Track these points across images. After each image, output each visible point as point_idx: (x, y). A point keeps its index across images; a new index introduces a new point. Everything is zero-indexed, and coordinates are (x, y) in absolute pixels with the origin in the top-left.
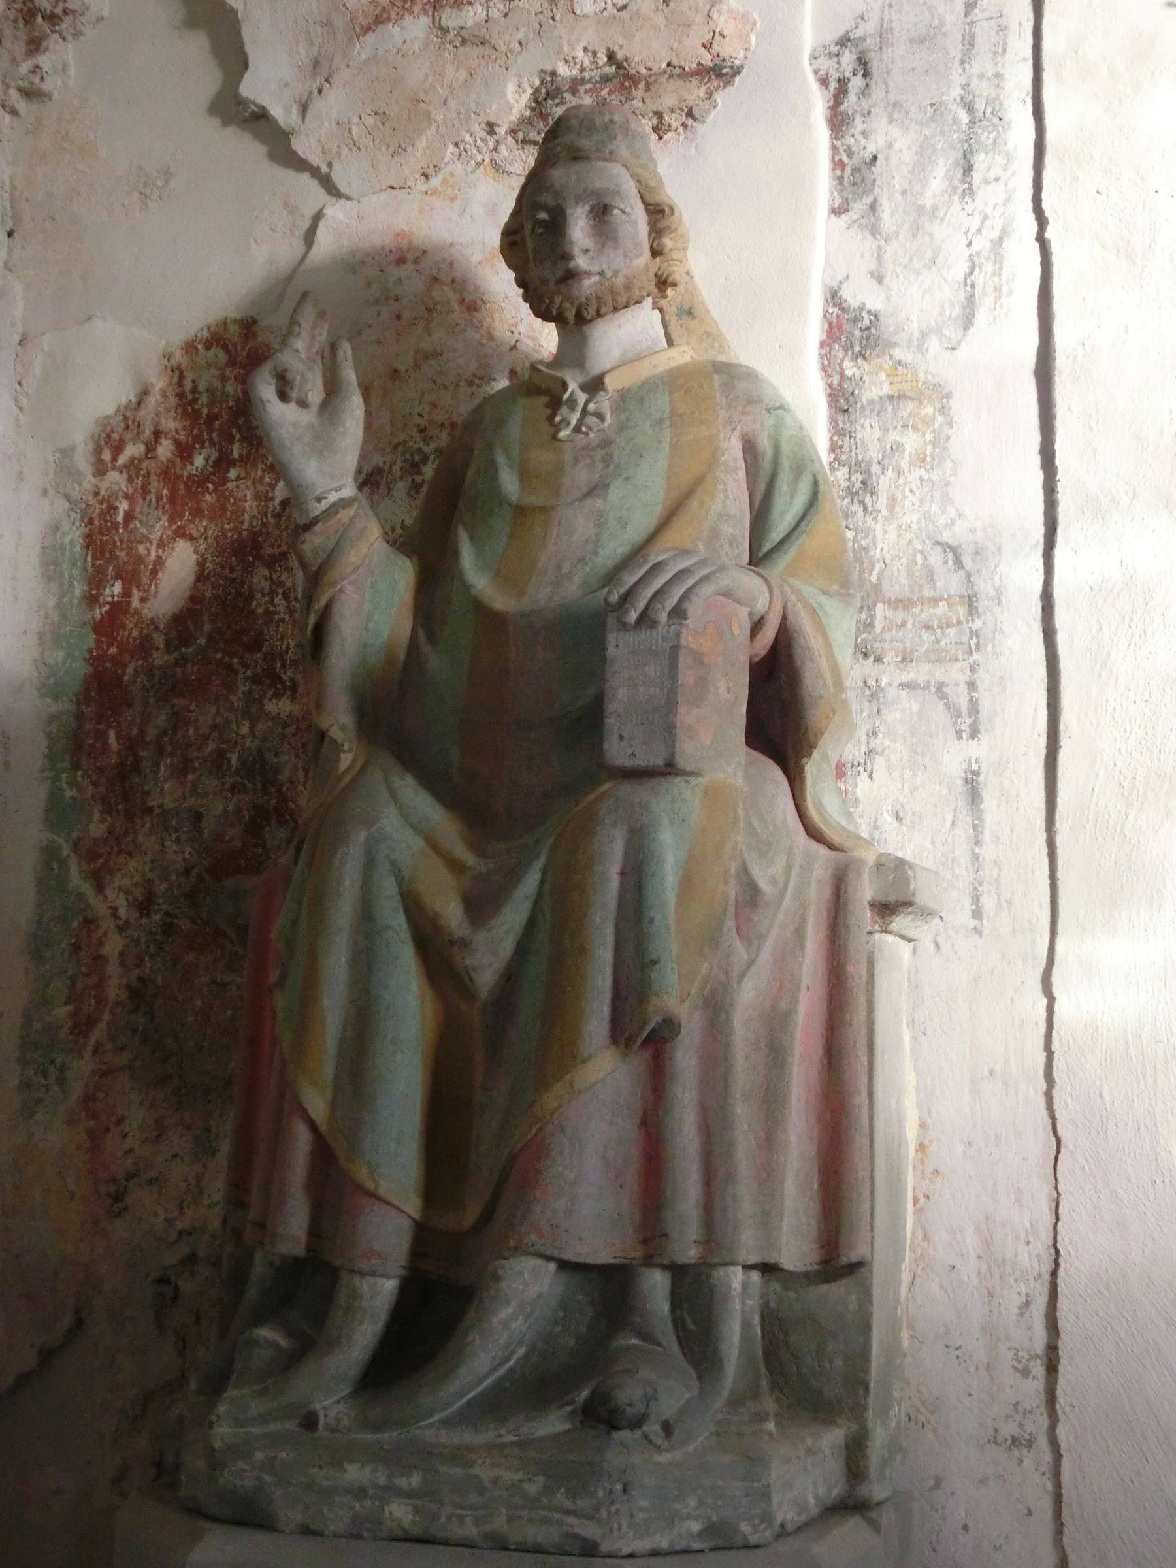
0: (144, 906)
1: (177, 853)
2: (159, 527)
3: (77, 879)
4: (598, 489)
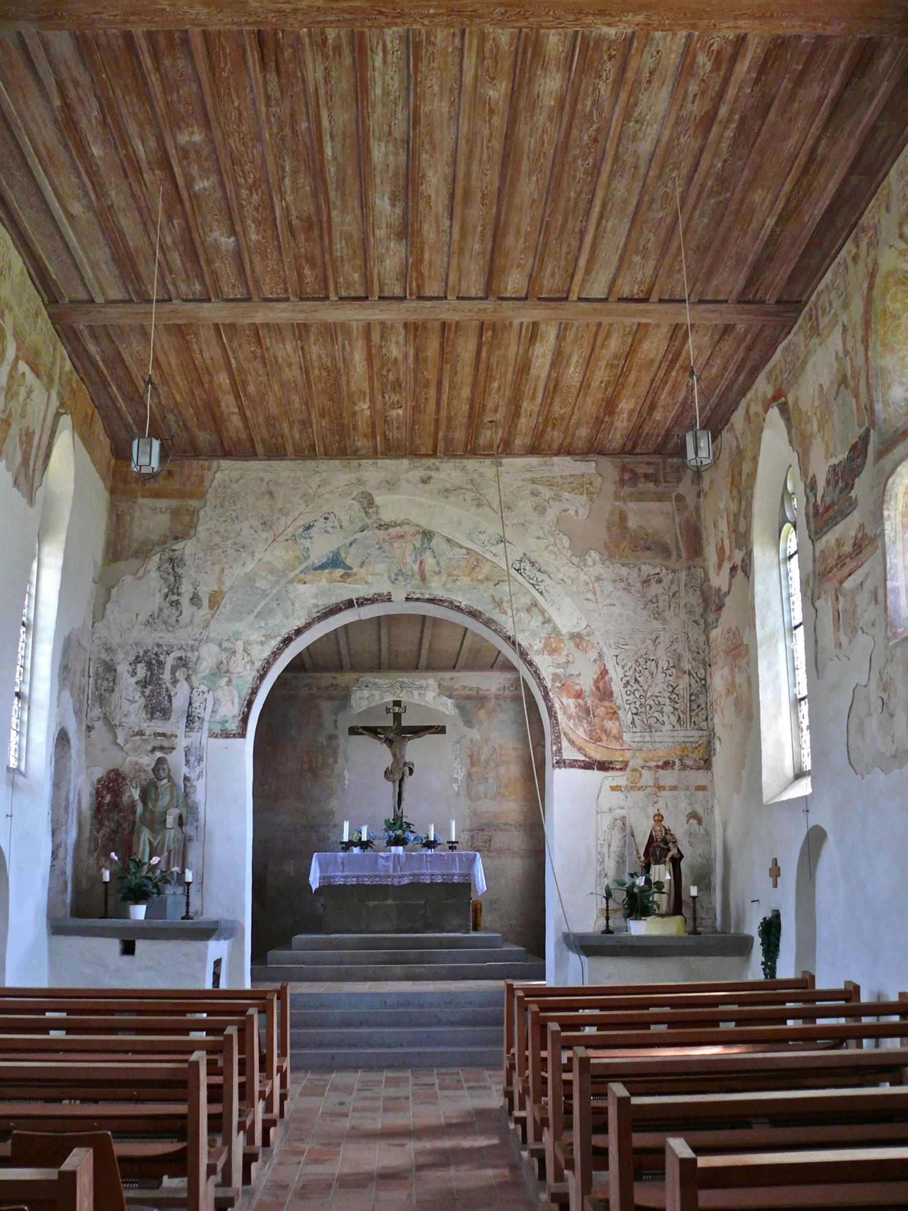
1: (108, 830)
3: (95, 832)
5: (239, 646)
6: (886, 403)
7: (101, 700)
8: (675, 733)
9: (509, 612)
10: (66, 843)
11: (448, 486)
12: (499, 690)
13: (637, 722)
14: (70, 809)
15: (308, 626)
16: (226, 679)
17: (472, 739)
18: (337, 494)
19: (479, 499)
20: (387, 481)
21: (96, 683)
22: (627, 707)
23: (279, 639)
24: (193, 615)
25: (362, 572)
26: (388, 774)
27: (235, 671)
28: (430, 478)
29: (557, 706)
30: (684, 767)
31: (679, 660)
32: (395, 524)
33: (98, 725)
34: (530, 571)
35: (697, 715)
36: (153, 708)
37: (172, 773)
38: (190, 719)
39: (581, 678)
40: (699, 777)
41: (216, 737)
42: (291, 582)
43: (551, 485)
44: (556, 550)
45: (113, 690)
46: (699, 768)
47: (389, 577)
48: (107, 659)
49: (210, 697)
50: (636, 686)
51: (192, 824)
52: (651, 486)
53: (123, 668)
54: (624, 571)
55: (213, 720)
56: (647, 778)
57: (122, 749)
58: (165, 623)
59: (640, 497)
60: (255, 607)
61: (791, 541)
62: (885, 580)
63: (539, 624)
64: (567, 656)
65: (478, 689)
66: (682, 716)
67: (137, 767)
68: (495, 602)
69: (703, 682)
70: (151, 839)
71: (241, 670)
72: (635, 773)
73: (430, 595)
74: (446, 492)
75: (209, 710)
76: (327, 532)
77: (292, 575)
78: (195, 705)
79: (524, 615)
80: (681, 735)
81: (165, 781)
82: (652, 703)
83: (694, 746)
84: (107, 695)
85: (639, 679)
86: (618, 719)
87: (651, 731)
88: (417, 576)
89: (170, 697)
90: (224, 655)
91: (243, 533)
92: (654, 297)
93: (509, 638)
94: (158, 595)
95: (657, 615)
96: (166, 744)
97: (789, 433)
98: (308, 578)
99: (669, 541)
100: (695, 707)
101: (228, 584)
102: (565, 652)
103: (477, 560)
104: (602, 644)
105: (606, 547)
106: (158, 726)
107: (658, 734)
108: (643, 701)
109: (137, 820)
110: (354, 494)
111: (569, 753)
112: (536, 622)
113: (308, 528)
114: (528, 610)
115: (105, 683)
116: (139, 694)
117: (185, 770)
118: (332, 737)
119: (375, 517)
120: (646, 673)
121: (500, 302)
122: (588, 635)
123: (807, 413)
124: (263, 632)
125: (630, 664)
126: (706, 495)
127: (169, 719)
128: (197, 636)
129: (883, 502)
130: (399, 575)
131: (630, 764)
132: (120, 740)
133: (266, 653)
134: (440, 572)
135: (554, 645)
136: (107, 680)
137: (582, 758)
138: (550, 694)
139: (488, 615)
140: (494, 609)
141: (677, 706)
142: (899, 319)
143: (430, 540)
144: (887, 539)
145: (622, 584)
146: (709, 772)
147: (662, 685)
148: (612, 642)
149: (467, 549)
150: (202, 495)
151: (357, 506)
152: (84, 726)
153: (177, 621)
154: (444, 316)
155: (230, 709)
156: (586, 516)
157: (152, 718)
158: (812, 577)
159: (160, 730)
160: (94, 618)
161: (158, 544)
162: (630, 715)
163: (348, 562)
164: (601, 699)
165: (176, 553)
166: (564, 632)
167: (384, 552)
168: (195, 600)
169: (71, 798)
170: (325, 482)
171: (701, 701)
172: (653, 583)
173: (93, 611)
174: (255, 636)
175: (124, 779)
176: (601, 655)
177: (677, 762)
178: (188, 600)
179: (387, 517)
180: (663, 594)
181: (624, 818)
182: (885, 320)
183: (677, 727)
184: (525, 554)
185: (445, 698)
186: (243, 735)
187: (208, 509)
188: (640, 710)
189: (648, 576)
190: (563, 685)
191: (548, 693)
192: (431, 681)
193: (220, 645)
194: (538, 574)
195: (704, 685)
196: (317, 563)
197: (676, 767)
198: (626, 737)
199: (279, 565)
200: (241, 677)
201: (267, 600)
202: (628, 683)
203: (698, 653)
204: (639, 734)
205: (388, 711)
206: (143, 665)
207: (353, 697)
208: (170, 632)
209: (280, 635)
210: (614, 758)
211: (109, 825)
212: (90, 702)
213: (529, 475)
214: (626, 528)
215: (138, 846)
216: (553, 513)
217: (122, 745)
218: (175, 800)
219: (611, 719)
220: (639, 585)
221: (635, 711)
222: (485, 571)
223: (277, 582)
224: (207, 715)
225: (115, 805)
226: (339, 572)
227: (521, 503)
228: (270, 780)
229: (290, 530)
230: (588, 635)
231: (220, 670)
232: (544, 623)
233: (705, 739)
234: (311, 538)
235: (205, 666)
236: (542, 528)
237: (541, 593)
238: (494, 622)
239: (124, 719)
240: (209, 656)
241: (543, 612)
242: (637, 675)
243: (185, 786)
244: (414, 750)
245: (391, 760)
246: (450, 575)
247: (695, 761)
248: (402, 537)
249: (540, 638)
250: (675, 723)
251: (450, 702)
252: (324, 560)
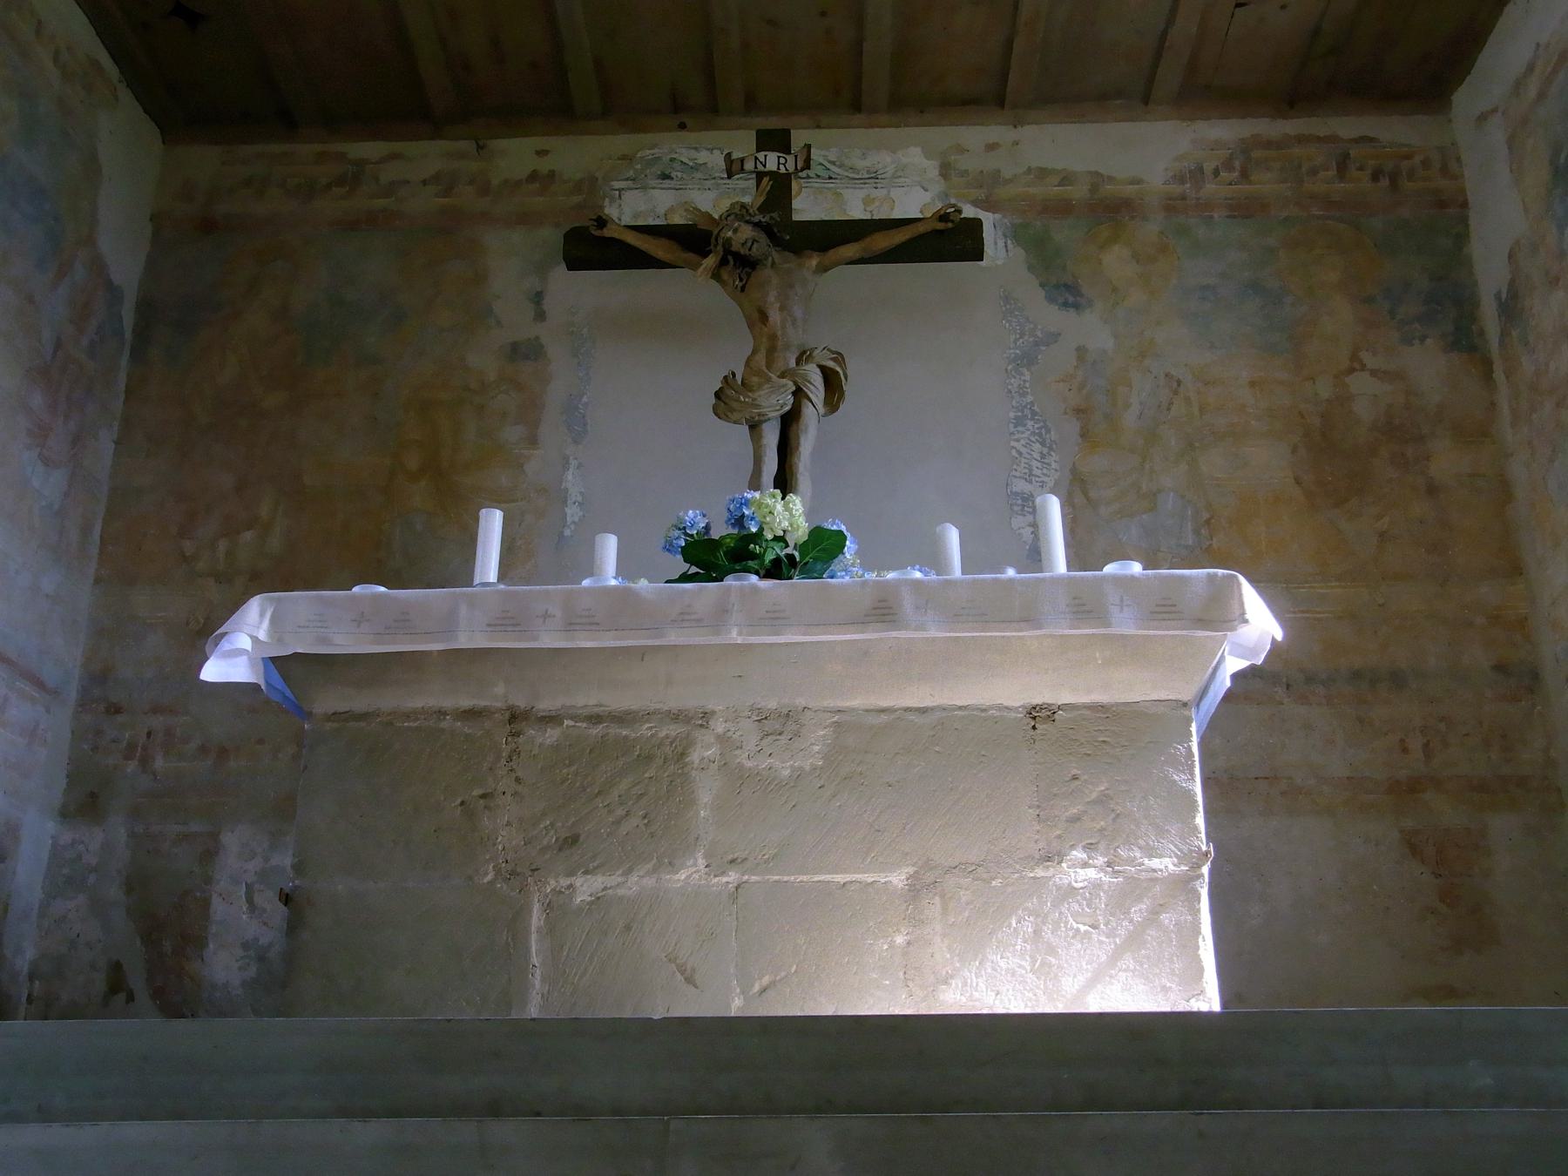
12: (1180, 179)
17: (1081, 351)
65: (1097, 180)
192: (914, 156)
228: (264, 511)
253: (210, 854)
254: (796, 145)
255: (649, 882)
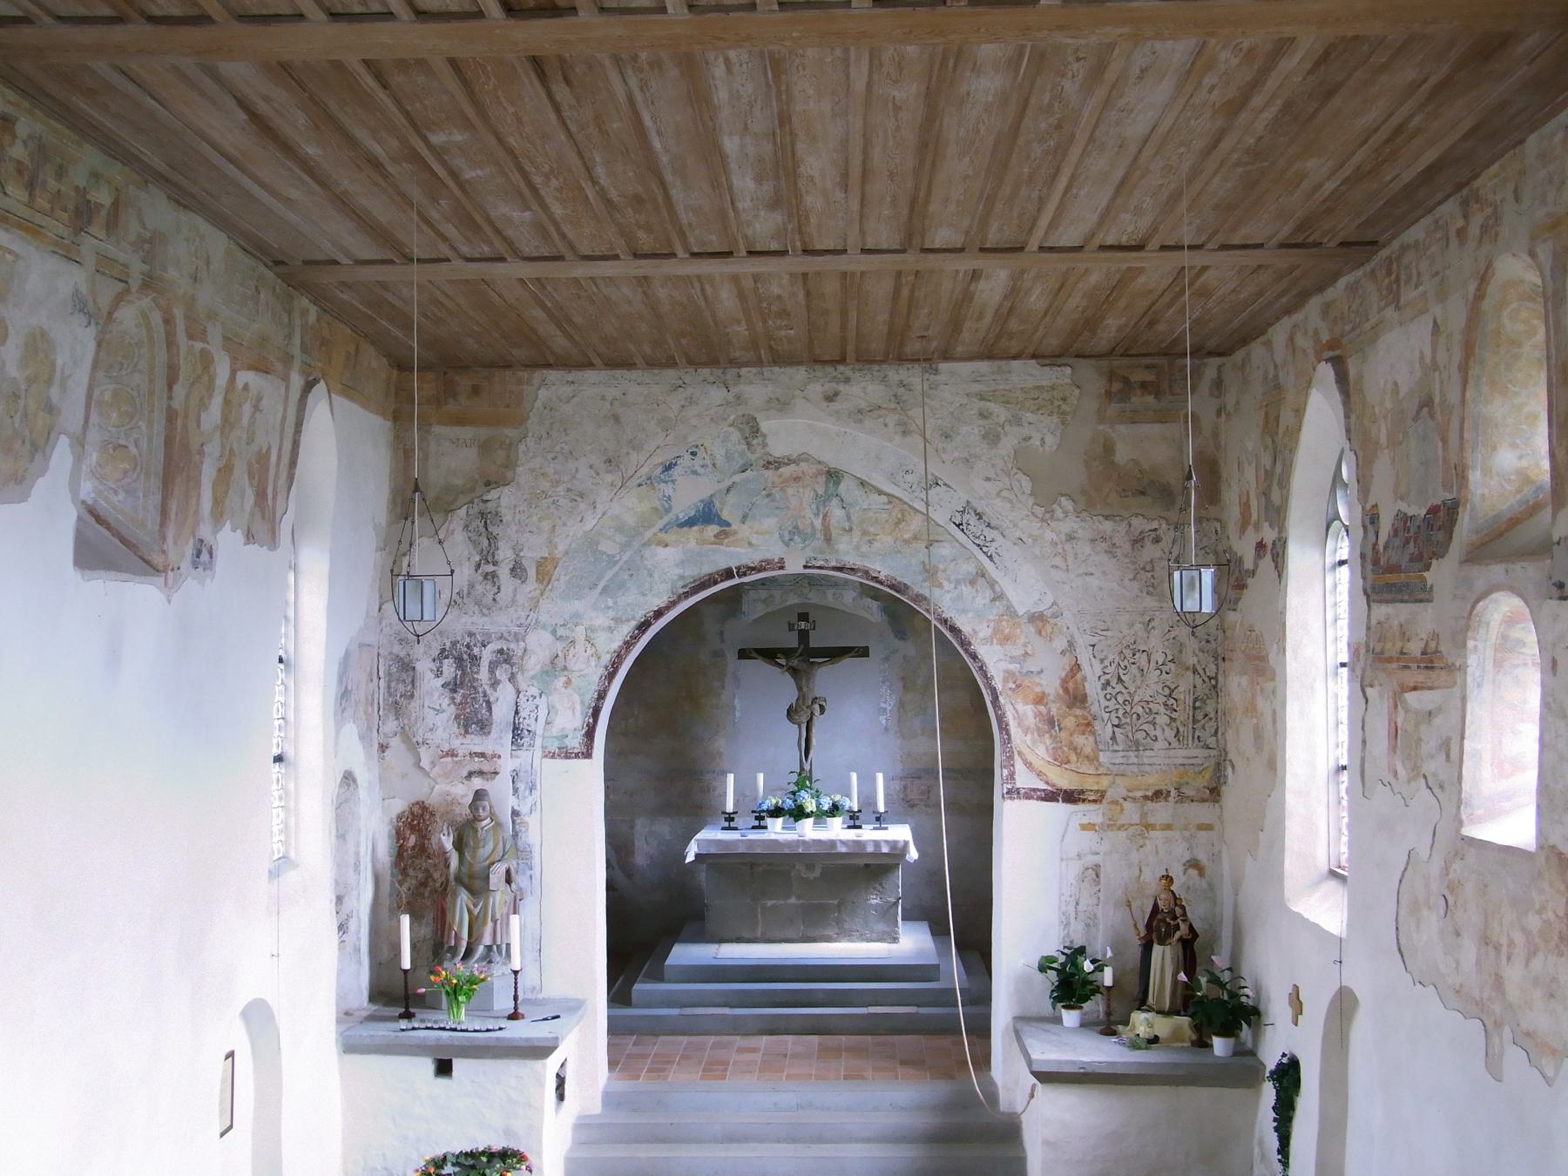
0: (409, 890)
1: (414, 882)
2: (409, 832)
4: (484, 846)
5: (580, 632)
6: (1487, 472)
7: (397, 709)
8: (1172, 753)
9: (946, 585)
10: (358, 911)
11: (863, 405)
13: (1117, 735)
14: (362, 867)
15: (672, 604)
16: (563, 679)
18: (708, 419)
19: (906, 424)
20: (777, 399)
21: (389, 687)
22: (1106, 716)
23: (634, 623)
24: (515, 590)
25: (744, 531)
26: (791, 713)
27: (576, 668)
28: (836, 394)
29: (1010, 716)
30: (1182, 798)
31: (1181, 652)
32: (790, 461)
33: (396, 743)
34: (975, 526)
35: (1203, 727)
36: (466, 720)
37: (497, 810)
38: (517, 732)
39: (1042, 675)
40: (1202, 812)
41: (553, 757)
42: (647, 544)
43: (1008, 402)
44: (1012, 497)
45: (412, 696)
46: (1204, 800)
47: (781, 537)
48: (402, 654)
49: (542, 703)
50: (1119, 688)
51: (524, 873)
52: (1150, 399)
53: (424, 666)
54: (1107, 526)
55: (547, 734)
56: (1131, 813)
57: (427, 774)
58: (478, 603)
59: (1134, 418)
60: (599, 579)
61: (1342, 548)
62: (1463, 738)
63: (987, 601)
64: (1025, 645)
66: (1181, 729)
67: (449, 799)
68: (927, 571)
69: (1213, 682)
70: (472, 907)
71: (583, 666)
72: (1114, 807)
73: (837, 561)
74: (859, 414)
75: (542, 720)
76: (695, 473)
77: (648, 534)
78: (522, 714)
79: (966, 590)
80: (1180, 755)
81: (488, 820)
82: (1140, 710)
83: (1197, 769)
84: (403, 701)
85: (1123, 677)
86: (1093, 733)
87: (1138, 750)
88: (819, 535)
89: (488, 703)
90: (559, 646)
91: (579, 476)
92: (1154, 244)
93: (946, 621)
94: (467, 564)
95: (1151, 589)
96: (486, 767)
97: (1347, 416)
98: (669, 538)
99: (1173, 482)
100: (1200, 716)
101: (561, 547)
102: (1022, 641)
103: (902, 511)
104: (1073, 629)
105: (1083, 492)
106: (476, 743)
107: (1147, 753)
108: (1128, 708)
109: (452, 877)
110: (732, 417)
111: (1025, 780)
112: (982, 599)
113: (668, 468)
114: (972, 583)
115: (401, 687)
116: (447, 701)
117: (512, 802)
118: (718, 654)
119: (760, 451)
120: (1134, 669)
121: (923, 255)
122: (1055, 616)
123: (1373, 407)
124: (611, 614)
125: (1111, 658)
126: (1229, 415)
127: (489, 733)
128: (523, 621)
129: (1467, 628)
130: (794, 533)
131: (1108, 795)
132: (425, 763)
133: (617, 644)
134: (851, 529)
135: (1007, 631)
136: (404, 681)
137: (1043, 786)
138: (1001, 698)
139: (917, 589)
140: (924, 581)
141: (1174, 715)
142: (1520, 346)
143: (837, 484)
144: (1469, 679)
145: (1104, 545)
146: (1217, 805)
147: (1153, 686)
148: (1087, 626)
149: (888, 495)
150: (521, 421)
151: (735, 435)
152: (376, 746)
153: (494, 600)
154: (843, 268)
155: (570, 720)
156: (1055, 448)
157: (467, 732)
158: (1363, 651)
159: (478, 749)
160: (381, 597)
161: (462, 493)
162: (1109, 728)
163: (725, 515)
164: (1070, 706)
165: (489, 505)
166: (1020, 613)
167: (773, 500)
168: (517, 570)
169: (362, 850)
170: (691, 401)
171: (1210, 709)
172: (1148, 543)
173: (380, 589)
174: (601, 620)
175: (432, 814)
176: (1071, 644)
177: (1173, 792)
178: (507, 571)
179: (778, 449)
180: (1161, 558)
181: (1098, 866)
182: (1498, 346)
183: (1175, 744)
184: (968, 502)
185: (869, 600)
186: (588, 755)
187: (530, 442)
188: (1124, 721)
189: (1141, 533)
190: (1018, 686)
191: (998, 697)
193: (554, 632)
194: (987, 531)
195: (1215, 687)
196: (683, 517)
197: (1170, 799)
198: (1103, 757)
199: (630, 520)
200: (584, 676)
201: (616, 568)
202: (1108, 683)
203: (1208, 642)
204: (1121, 754)
205: (791, 627)
206: (452, 661)
207: (745, 599)
208: (484, 615)
209: (633, 618)
210: (1087, 786)
211: (416, 875)
212: (381, 713)
213: (976, 388)
214: (1113, 462)
215: (454, 916)
216: (1008, 443)
217: (427, 769)
218: (501, 845)
219: (1084, 734)
220: (1127, 546)
221: (1116, 723)
222: (912, 527)
223: (628, 545)
224: (539, 728)
225: (422, 849)
226: (712, 530)
227: (965, 429)
229: (644, 470)
230: (1055, 616)
231: (555, 667)
232: (994, 600)
233: (1213, 761)
234: (673, 481)
235: (534, 663)
236: (993, 466)
237: (990, 557)
238: (925, 599)
239: (428, 735)
240: (539, 646)
241: (992, 584)
242: (1121, 671)
243: (513, 822)
244: (826, 678)
245: (795, 694)
246: (865, 533)
247: (1198, 790)
248: (797, 479)
249: (989, 621)
250: (1173, 740)
251: (875, 605)
252: (692, 513)
253: (632, 827)
254: (811, 620)
255: (782, 902)
